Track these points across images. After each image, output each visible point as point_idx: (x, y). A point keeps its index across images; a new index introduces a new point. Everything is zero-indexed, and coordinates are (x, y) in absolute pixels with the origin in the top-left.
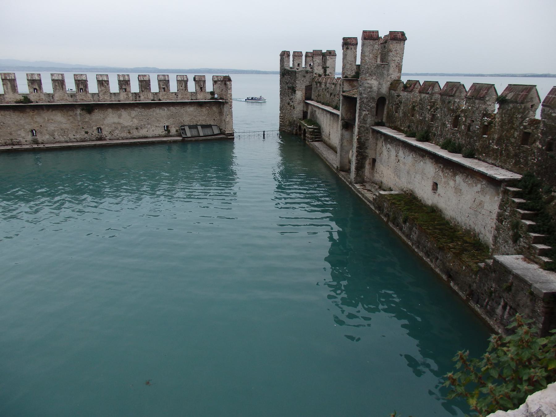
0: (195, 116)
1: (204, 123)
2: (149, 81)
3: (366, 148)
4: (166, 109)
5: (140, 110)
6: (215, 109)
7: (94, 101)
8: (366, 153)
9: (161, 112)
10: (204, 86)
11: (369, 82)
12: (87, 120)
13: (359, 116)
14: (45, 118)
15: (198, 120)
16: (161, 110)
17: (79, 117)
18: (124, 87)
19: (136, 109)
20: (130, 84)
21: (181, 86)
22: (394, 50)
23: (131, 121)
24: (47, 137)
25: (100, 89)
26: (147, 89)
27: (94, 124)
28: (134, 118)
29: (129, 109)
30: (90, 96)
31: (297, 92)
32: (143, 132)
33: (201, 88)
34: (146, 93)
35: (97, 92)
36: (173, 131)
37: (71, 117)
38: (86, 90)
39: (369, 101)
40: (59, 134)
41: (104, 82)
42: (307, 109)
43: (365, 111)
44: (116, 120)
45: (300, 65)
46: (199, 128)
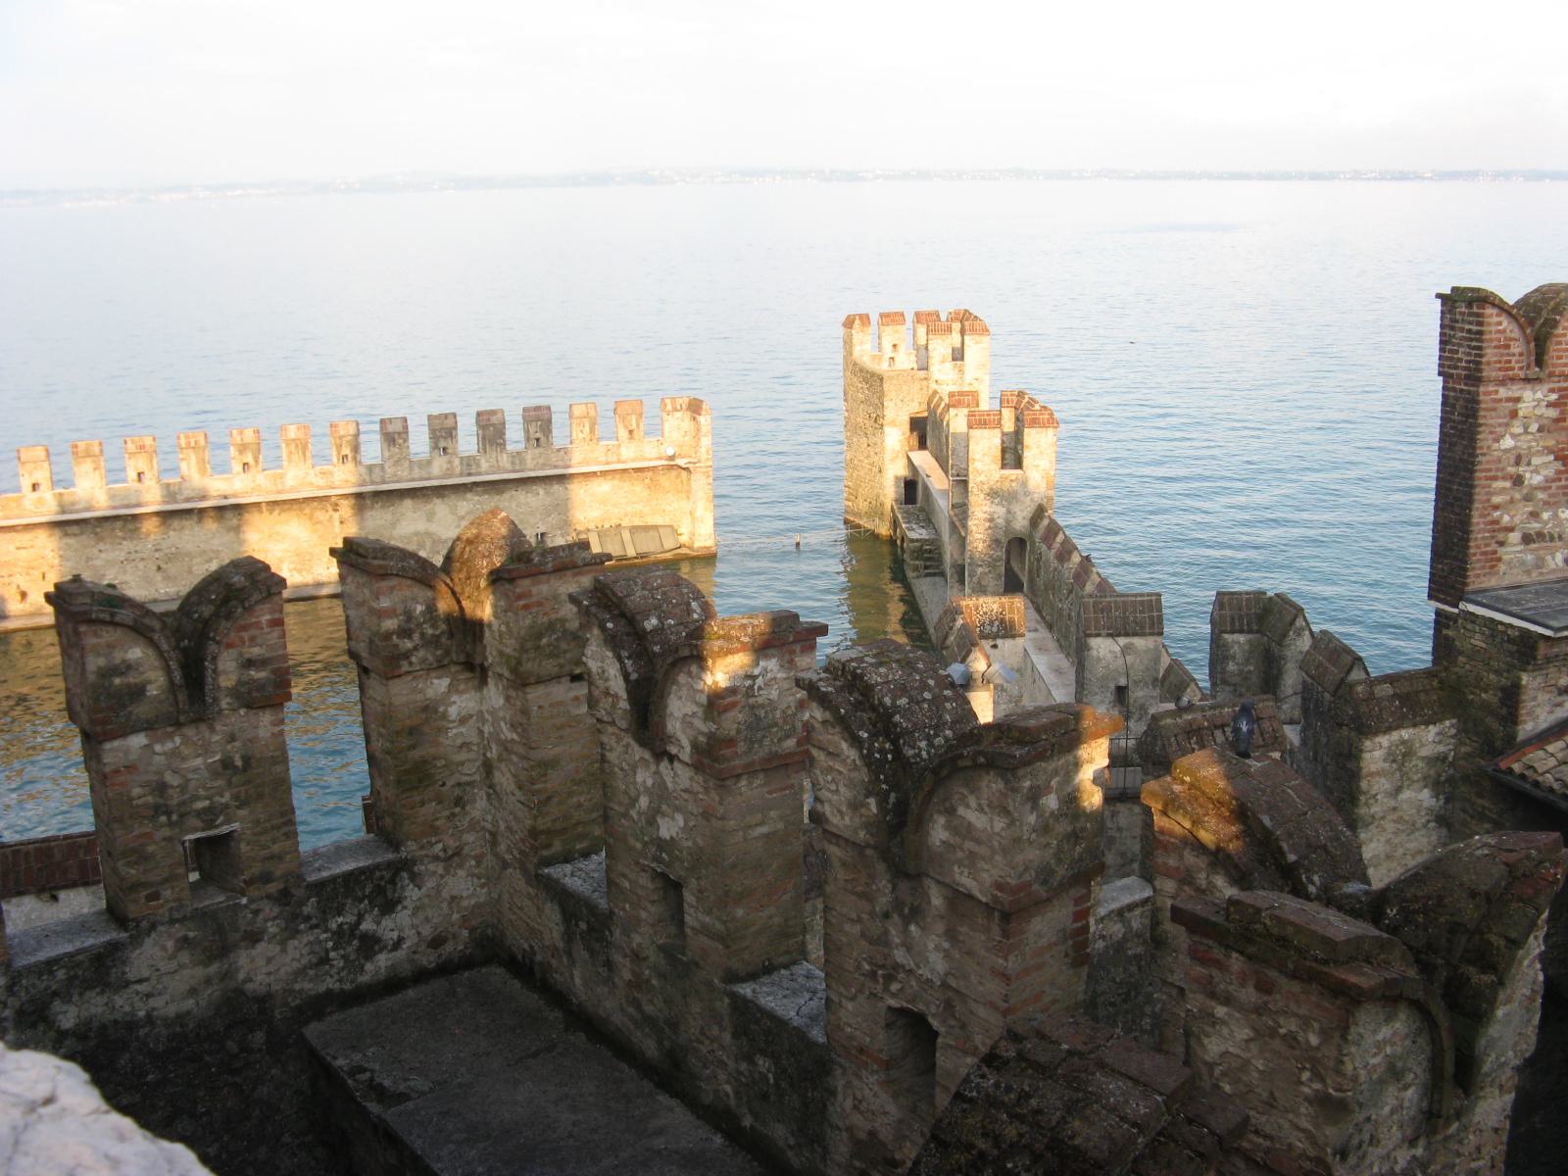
1: (637, 522)
2: (504, 424)
4: (541, 492)
7: (373, 483)
9: (529, 500)
18: (442, 444)
19: (469, 496)
20: (456, 434)
25: (387, 454)
26: (497, 444)
29: (453, 496)
31: (887, 429)
34: (494, 456)
35: (379, 461)
41: (396, 436)
44: (421, 526)
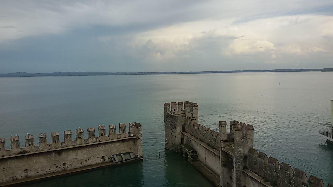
0: (120, 148)
3: (240, 181)
4: (103, 147)
5: (88, 149)
6: (131, 142)
8: (240, 183)
10: (125, 130)
11: (239, 149)
12: (58, 159)
13: (236, 166)
14: (34, 161)
15: (121, 150)
16: (100, 147)
17: (53, 158)
19: (86, 149)
21: (112, 132)
22: (249, 134)
23: (83, 156)
24: (34, 172)
27: (61, 161)
28: (85, 154)
30: (60, 144)
31: (177, 128)
32: (89, 162)
33: (123, 131)
36: (107, 159)
37: (49, 159)
38: (58, 142)
39: (240, 158)
40: (41, 170)
42: (184, 137)
43: (238, 163)
45: (176, 110)
46: (122, 155)
